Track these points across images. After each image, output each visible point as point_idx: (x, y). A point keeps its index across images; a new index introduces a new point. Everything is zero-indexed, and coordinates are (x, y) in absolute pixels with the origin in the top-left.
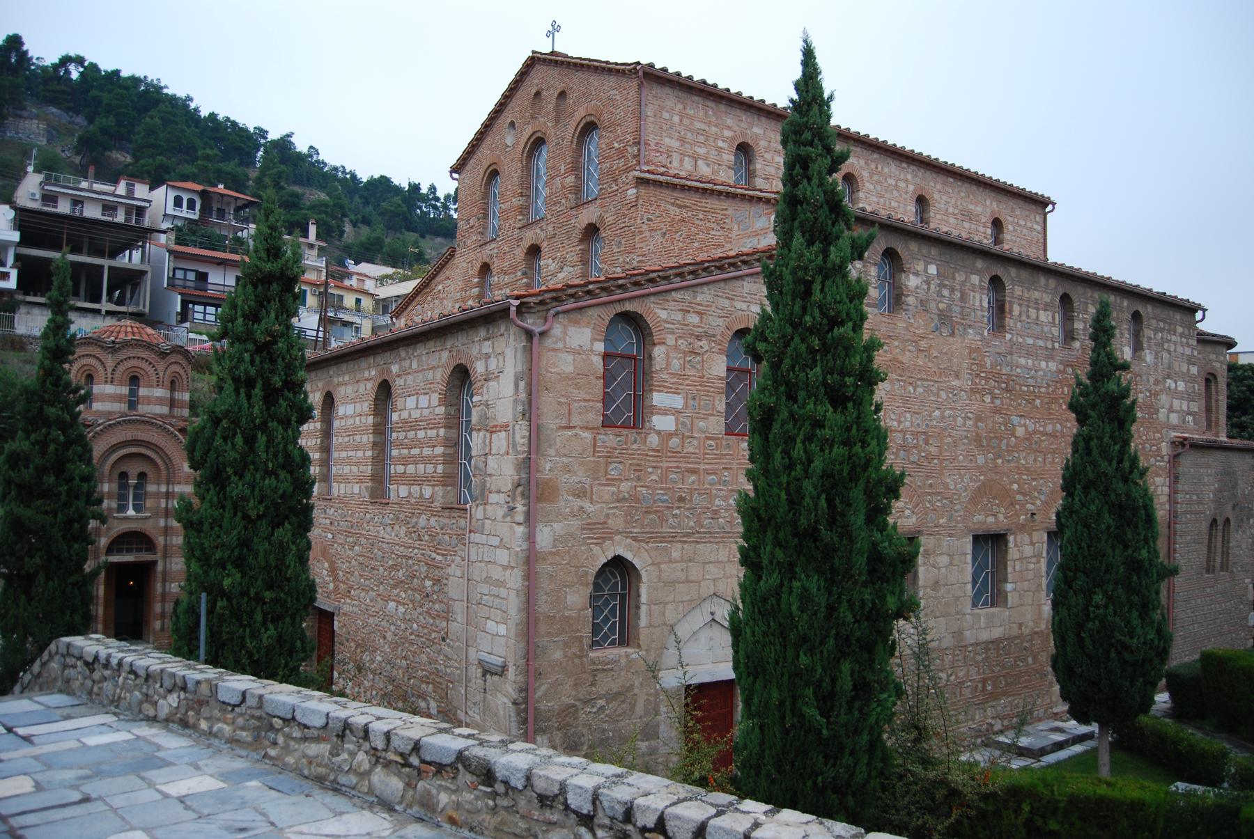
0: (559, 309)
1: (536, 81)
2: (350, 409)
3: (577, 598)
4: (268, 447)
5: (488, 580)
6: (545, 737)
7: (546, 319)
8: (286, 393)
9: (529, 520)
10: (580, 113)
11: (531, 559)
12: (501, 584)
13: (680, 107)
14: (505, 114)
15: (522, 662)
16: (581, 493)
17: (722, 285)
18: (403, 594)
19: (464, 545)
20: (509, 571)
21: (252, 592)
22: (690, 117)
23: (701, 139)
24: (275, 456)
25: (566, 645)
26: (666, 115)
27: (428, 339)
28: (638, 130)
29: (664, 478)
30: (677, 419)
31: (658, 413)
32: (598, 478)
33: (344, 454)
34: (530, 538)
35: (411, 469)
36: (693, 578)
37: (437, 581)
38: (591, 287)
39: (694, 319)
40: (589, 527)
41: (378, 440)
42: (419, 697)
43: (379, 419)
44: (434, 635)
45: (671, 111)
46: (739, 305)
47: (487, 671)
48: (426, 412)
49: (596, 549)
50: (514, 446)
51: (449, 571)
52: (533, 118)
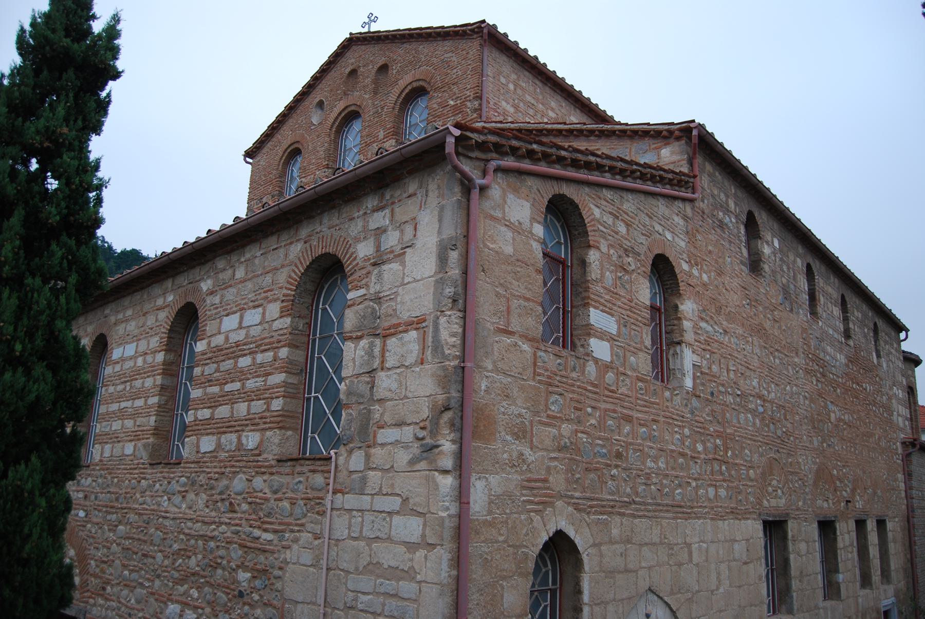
0: (501, 163)
1: (350, 61)
2: (130, 350)
3: (515, 595)
4: (18, 318)
5: (373, 568)
7: (484, 173)
8: (64, 238)
9: (461, 468)
10: (408, 79)
11: (461, 530)
12: (409, 574)
13: (514, 76)
14: (312, 96)
16: (521, 433)
17: (642, 197)
18: (195, 593)
20: (420, 554)
22: (522, 89)
23: (531, 112)
24: (30, 334)
26: (503, 80)
27: (266, 236)
28: (480, 86)
29: (601, 426)
30: (611, 347)
31: (596, 337)
32: (537, 413)
33: (114, 407)
34: (462, 495)
35: (223, 411)
36: (631, 566)
37: (260, 572)
38: (535, 146)
39: (622, 229)
40: (529, 485)
43: (171, 357)
46: (658, 228)
48: (255, 331)
49: (537, 518)
50: (438, 347)
51: (288, 555)
52: (345, 94)
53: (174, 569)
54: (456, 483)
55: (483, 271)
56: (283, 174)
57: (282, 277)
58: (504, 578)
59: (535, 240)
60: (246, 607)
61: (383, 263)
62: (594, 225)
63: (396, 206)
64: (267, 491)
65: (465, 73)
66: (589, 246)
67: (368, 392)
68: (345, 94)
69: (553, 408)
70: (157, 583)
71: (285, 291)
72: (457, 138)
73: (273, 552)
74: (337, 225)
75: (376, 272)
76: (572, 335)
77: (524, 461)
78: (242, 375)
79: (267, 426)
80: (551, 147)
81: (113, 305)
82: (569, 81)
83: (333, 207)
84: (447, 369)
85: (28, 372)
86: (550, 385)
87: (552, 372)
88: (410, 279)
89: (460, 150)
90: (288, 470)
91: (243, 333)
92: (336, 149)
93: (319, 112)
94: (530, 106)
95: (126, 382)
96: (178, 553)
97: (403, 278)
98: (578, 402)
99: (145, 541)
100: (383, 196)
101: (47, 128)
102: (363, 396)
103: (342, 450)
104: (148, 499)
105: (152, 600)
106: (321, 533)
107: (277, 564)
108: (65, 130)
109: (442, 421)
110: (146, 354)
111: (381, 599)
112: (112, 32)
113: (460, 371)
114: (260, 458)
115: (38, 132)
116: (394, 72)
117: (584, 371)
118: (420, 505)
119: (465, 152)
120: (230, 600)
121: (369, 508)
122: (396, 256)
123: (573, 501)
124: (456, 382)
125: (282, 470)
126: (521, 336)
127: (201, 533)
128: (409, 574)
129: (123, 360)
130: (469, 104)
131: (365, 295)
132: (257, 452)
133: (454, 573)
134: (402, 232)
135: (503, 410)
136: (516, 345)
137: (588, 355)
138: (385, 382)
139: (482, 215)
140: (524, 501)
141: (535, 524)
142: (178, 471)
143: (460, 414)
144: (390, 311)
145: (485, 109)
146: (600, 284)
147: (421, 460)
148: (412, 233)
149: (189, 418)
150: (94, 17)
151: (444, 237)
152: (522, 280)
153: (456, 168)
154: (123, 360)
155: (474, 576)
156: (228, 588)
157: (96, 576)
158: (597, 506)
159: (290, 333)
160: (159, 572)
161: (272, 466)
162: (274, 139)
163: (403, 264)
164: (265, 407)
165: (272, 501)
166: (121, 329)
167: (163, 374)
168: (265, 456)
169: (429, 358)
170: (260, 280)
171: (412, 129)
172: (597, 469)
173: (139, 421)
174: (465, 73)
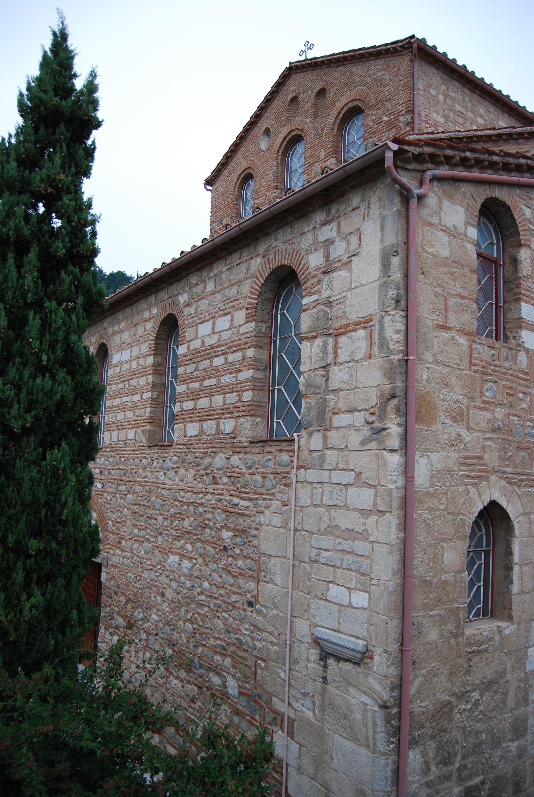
0: (437, 172)
1: (291, 89)
2: (126, 355)
3: (454, 555)
4: (42, 335)
5: (332, 529)
6: (417, 751)
7: (421, 183)
8: (70, 267)
9: (406, 446)
10: (344, 100)
11: (407, 500)
12: (364, 535)
13: (443, 87)
14: (259, 124)
15: (394, 647)
16: (459, 417)
18: (189, 547)
19: (289, 485)
20: (372, 519)
21: (11, 539)
22: (452, 99)
23: (461, 120)
24: (52, 347)
25: (443, 621)
28: (412, 100)
32: (472, 399)
33: (117, 402)
34: (407, 470)
35: (204, 403)
38: (468, 154)
40: (466, 461)
41: (157, 380)
42: (209, 669)
43: (159, 359)
44: (234, 598)
45: (437, 89)
47: (327, 653)
48: (226, 336)
49: (473, 491)
50: (383, 343)
51: (262, 518)
52: (288, 120)
53: (172, 528)
54: (402, 460)
55: (423, 273)
56: (238, 198)
57: (246, 288)
58: (444, 540)
59: (469, 242)
60: (230, 559)
61: (332, 271)
62: (524, 225)
63: (341, 219)
64: (242, 467)
65: (397, 89)
66: (520, 245)
67: (324, 384)
68: (288, 120)
69: (487, 394)
70: (160, 538)
71: (249, 300)
72: (395, 153)
73: (249, 516)
74: (290, 240)
75: (326, 279)
76: (504, 328)
77: (461, 441)
78: (217, 373)
79: (240, 414)
80: (484, 153)
81: (109, 319)
82: (497, 87)
83: (286, 224)
84: (393, 363)
85: (53, 377)
86: (485, 373)
87: (486, 362)
88: (357, 284)
89: (398, 163)
90: (258, 450)
91: (216, 337)
92: (283, 171)
93: (267, 139)
94: (460, 114)
95: (125, 381)
96: (174, 516)
97: (351, 284)
98: (510, 388)
99: (149, 507)
100: (329, 210)
101: (49, 176)
102: (319, 388)
103: (303, 433)
104: (149, 474)
105: (157, 552)
106: (288, 501)
107: (253, 525)
108: (63, 176)
109: (389, 408)
110: (139, 358)
111: (340, 555)
112: (91, 87)
113: (404, 363)
114: (235, 441)
115: (42, 180)
116: (332, 94)
117: (516, 360)
118: (371, 479)
119: (403, 165)
120: (217, 553)
121: (328, 481)
122: (343, 264)
123: (505, 475)
124: (400, 373)
125: (254, 450)
126: (458, 331)
127: (192, 500)
128: (364, 535)
129: (121, 363)
130: (401, 118)
131: (317, 300)
132: (233, 435)
133: (402, 535)
134: (348, 242)
135: (442, 396)
136: (453, 339)
137: (519, 345)
138: (338, 375)
139: (420, 222)
140: (462, 475)
141: (471, 495)
142: (171, 451)
143: (404, 401)
144: (340, 313)
145: (417, 122)
146: (531, 280)
147: (371, 441)
148: (357, 242)
149: (177, 409)
150: (75, 76)
151: (387, 244)
152: (458, 280)
153: (395, 181)
154: (121, 364)
155: (419, 538)
156: (215, 544)
157: (113, 533)
158: (527, 480)
159: (255, 336)
160: (161, 530)
161: (246, 447)
162: (229, 167)
163: (350, 271)
164: (237, 398)
165: (247, 475)
166: (117, 338)
167: (153, 373)
168: (239, 438)
169: (376, 353)
170: (227, 291)
171: (350, 146)
172: (527, 448)
173: (137, 412)
174: (397, 89)
